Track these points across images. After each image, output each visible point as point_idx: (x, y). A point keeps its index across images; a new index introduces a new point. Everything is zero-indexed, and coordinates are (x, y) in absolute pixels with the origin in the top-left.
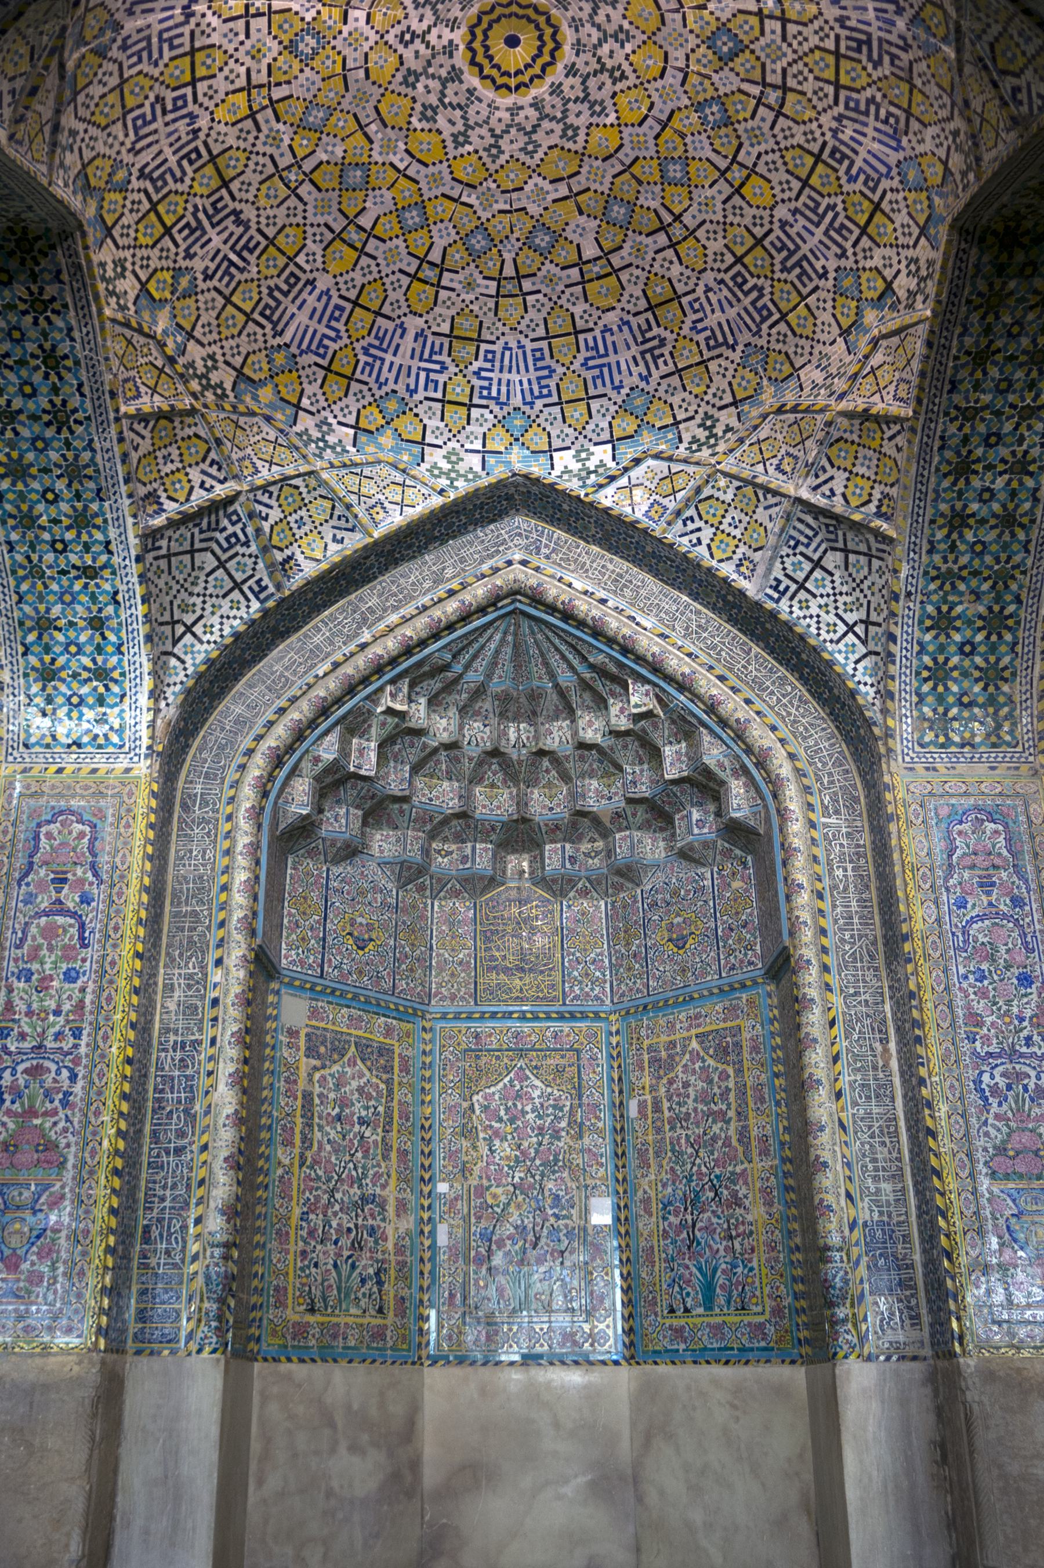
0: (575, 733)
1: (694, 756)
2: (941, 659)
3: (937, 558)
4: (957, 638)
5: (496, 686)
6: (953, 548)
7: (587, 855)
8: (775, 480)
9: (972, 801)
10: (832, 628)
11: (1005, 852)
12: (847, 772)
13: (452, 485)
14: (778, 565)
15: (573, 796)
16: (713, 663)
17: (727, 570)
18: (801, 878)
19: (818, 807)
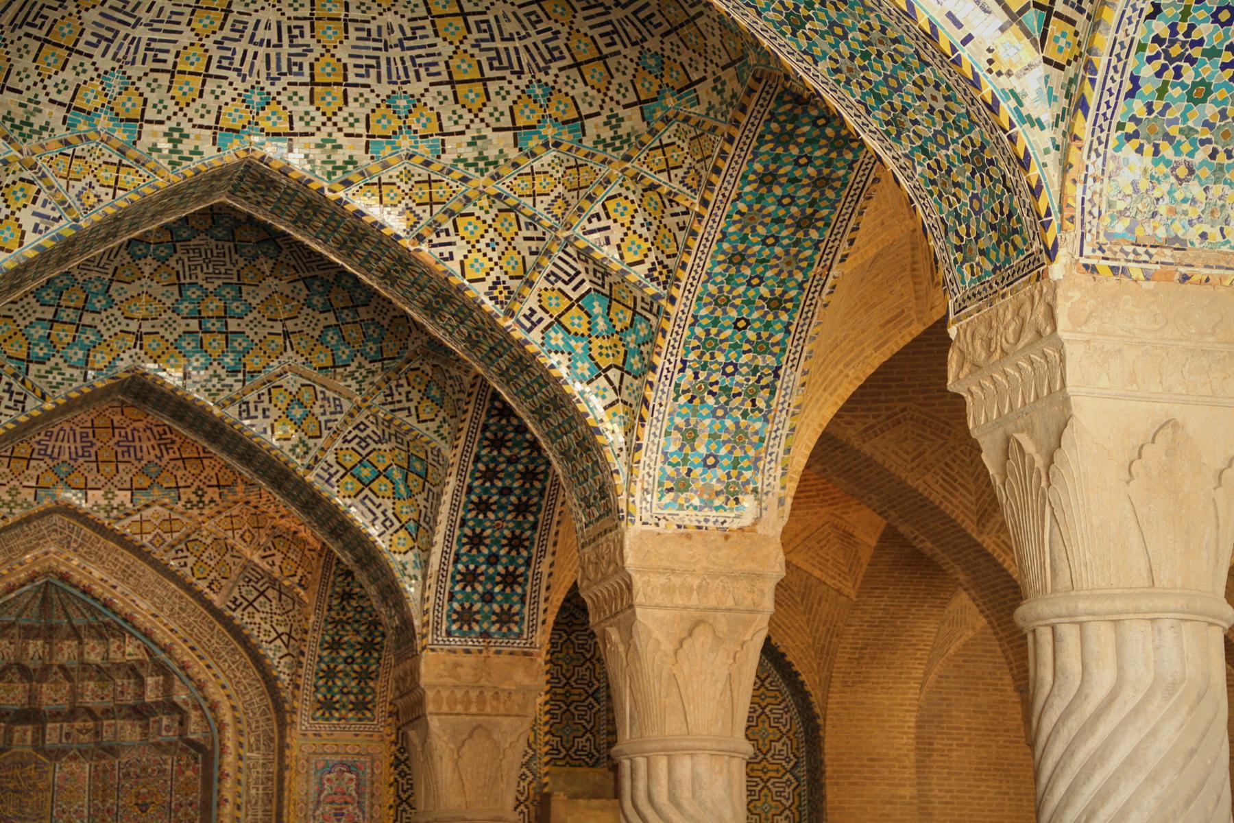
0: (81, 654)
1: (168, 689)
2: (332, 666)
3: (333, 613)
4: (344, 654)
5: (23, 621)
6: (343, 608)
7: (80, 731)
8: (240, 545)
9: (339, 758)
10: (267, 633)
11: (354, 793)
12: (268, 719)
13: (11, 513)
14: (236, 589)
15: (74, 694)
16: (188, 637)
17: (202, 585)
18: (228, 795)
19: (246, 745)
